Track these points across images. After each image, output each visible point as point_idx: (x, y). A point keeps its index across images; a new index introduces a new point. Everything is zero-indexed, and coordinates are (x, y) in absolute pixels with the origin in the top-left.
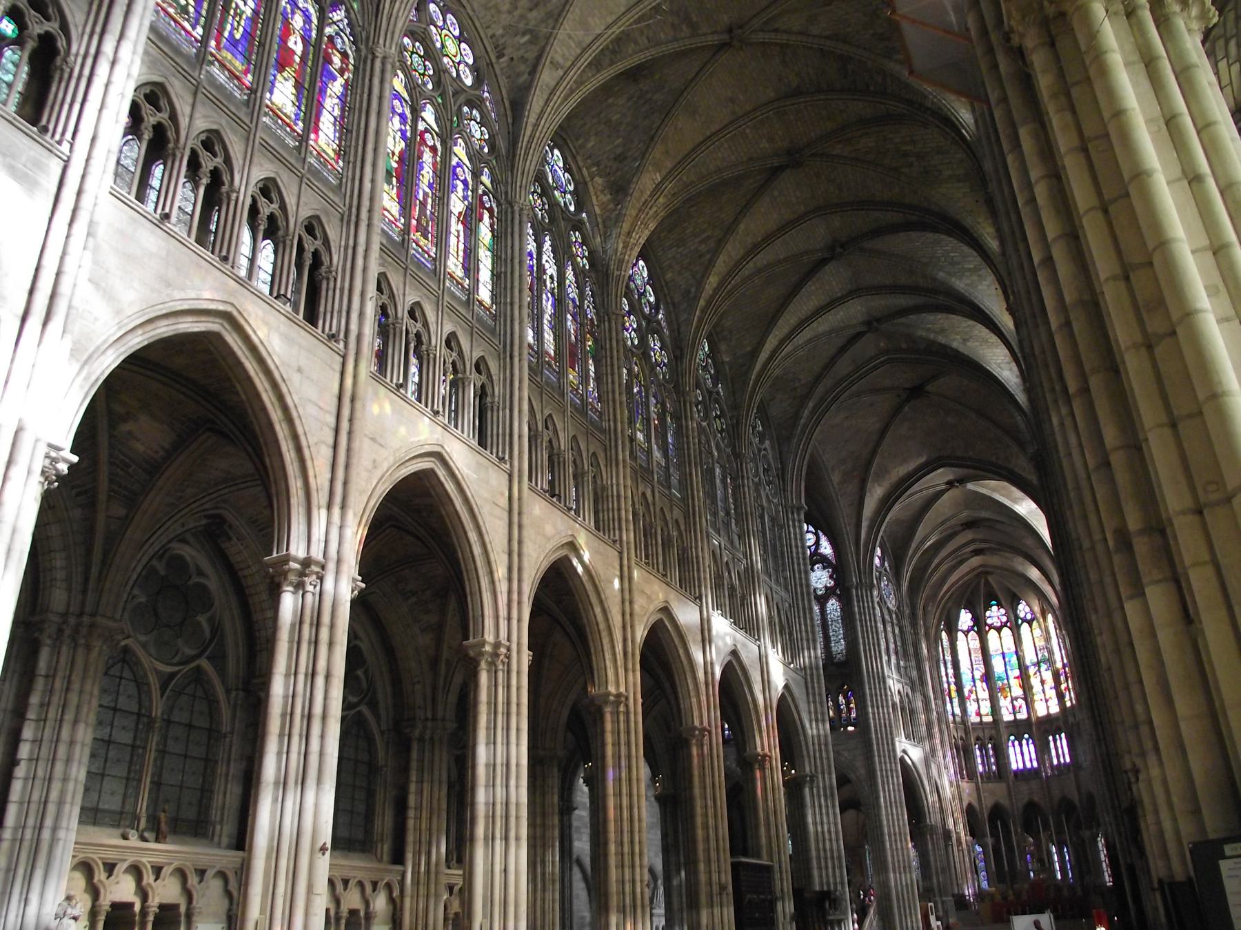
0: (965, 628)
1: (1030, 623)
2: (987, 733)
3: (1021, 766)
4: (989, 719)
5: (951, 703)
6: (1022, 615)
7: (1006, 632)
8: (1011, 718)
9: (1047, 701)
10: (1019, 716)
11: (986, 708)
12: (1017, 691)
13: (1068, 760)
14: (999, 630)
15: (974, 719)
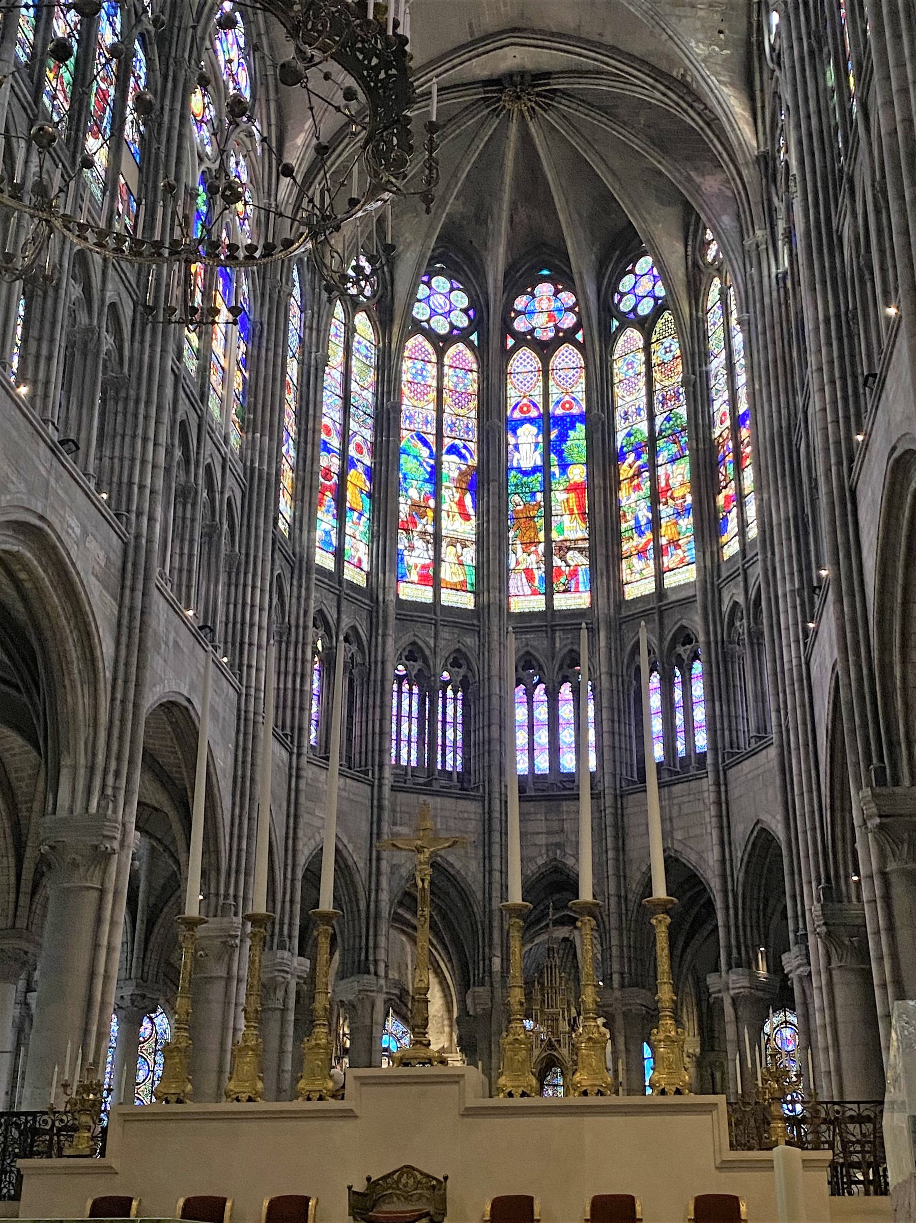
0: (441, 326)
1: (646, 325)
2: (447, 640)
3: (542, 764)
4: (467, 601)
5: (341, 517)
6: (626, 305)
7: (567, 358)
8: (538, 604)
9: (659, 552)
10: (562, 602)
11: (459, 564)
12: (571, 528)
13: (701, 740)
14: (545, 350)
15: (413, 591)
